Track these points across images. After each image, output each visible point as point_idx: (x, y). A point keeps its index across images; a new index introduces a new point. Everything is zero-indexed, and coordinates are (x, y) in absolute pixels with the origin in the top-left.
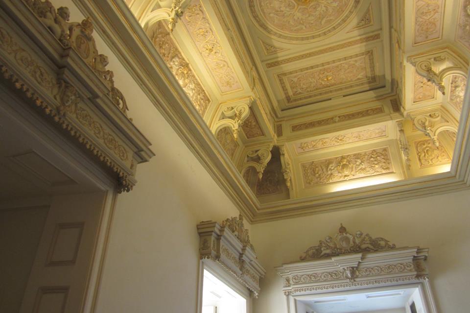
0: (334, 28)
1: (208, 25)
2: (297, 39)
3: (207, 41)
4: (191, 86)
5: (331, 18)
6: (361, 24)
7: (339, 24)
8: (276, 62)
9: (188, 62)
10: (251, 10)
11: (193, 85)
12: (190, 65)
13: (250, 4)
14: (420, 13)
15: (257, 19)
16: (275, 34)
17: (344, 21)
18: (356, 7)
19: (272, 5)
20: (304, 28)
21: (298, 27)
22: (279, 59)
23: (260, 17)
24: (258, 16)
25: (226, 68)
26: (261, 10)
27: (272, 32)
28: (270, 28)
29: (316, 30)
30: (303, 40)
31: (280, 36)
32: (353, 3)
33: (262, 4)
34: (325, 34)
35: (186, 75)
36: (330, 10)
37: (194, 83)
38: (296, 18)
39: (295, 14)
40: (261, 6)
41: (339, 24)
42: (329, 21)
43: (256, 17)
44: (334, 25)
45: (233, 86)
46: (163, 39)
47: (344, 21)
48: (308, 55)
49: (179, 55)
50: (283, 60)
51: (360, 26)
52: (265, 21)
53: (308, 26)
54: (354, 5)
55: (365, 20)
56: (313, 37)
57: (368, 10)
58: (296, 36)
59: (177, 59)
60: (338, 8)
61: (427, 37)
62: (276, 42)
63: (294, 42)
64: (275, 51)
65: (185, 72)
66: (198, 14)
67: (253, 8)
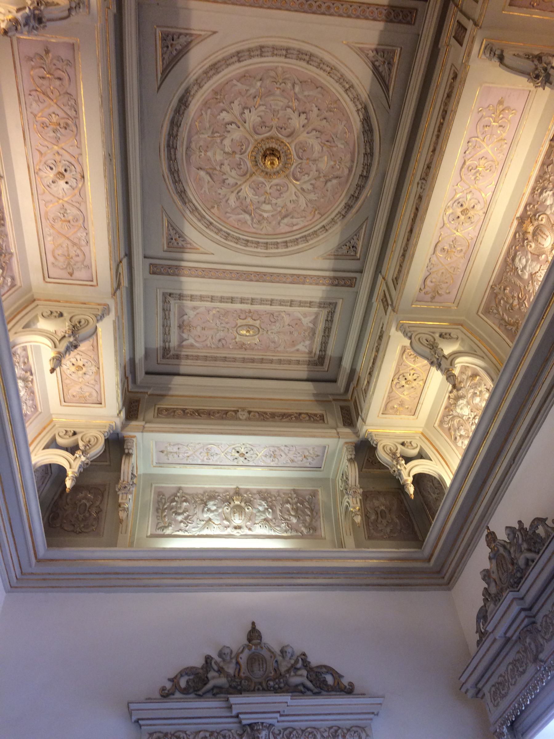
0: (239, 56)
1: (434, 259)
2: (321, 64)
3: (457, 234)
4: (549, 202)
5: (240, 86)
6: (183, 40)
7: (226, 61)
8: (391, 21)
9: (515, 223)
10: (368, 171)
11: (544, 195)
12: (518, 215)
13: (365, 183)
14: (70, 125)
15: (369, 150)
16: (356, 99)
17: (215, 68)
18: (187, 91)
19: (332, 163)
20: (297, 89)
21: (306, 93)
22: (380, 25)
23: (363, 151)
24: (365, 154)
25: (468, 163)
26: (353, 161)
27: (360, 107)
28: (358, 119)
29: (277, 67)
30: (311, 55)
31: (349, 89)
32: (193, 102)
33: (346, 171)
34: (261, 50)
35: (536, 223)
36: (236, 108)
37: (544, 189)
38: (303, 116)
39: (302, 129)
40: (350, 170)
41: (226, 61)
42: (243, 77)
43: (369, 154)
44: (238, 65)
45: (495, 102)
46: (502, 302)
47: (215, 68)
48: (314, 8)
49: (512, 252)
50: (375, 19)
51: (186, 35)
52: (358, 138)
53: (289, 85)
54: (190, 99)
55: (175, 47)
56: (287, 52)
57: (166, 71)
58: (321, 72)
59: (517, 260)
60: (221, 104)
61: (47, 52)
62: (361, 75)
63: (327, 58)
64: (377, 53)
65: (531, 229)
66: (432, 282)
67: (365, 174)
